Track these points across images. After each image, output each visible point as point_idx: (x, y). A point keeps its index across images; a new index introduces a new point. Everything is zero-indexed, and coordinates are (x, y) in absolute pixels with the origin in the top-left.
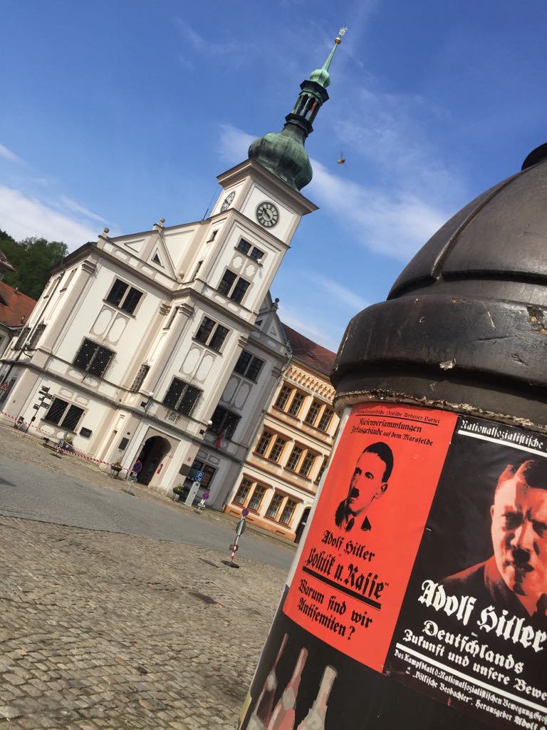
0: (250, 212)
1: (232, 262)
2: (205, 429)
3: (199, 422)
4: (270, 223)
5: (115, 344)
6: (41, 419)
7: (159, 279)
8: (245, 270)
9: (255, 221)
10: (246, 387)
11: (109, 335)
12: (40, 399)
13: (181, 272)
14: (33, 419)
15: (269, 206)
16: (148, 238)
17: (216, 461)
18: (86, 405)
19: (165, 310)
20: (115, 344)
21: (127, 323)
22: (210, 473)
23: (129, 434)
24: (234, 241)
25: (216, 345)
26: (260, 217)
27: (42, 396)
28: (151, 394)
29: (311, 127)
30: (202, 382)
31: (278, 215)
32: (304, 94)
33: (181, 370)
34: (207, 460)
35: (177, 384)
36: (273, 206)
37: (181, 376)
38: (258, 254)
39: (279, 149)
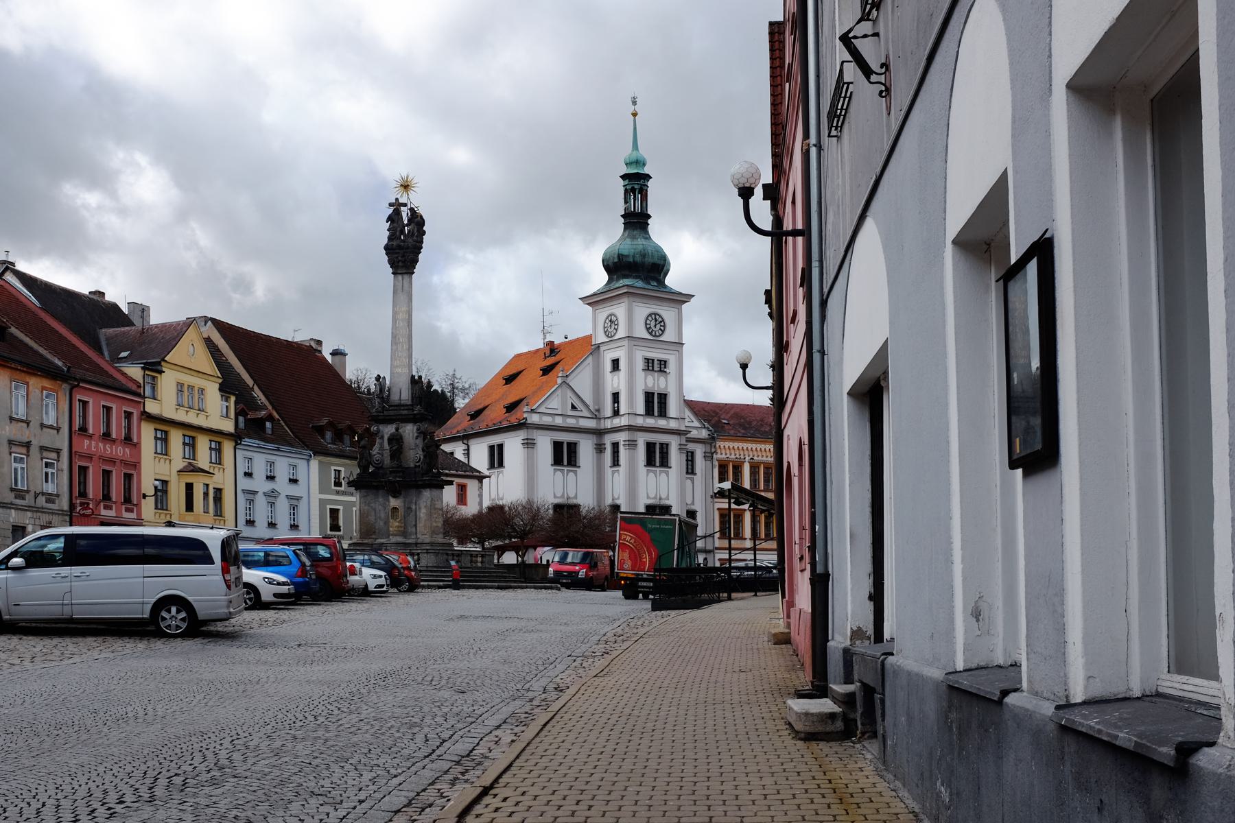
0: (641, 332)
5: (576, 497)
7: (585, 423)
24: (640, 364)
25: (665, 463)
33: (648, 497)
36: (655, 314)
39: (638, 259)
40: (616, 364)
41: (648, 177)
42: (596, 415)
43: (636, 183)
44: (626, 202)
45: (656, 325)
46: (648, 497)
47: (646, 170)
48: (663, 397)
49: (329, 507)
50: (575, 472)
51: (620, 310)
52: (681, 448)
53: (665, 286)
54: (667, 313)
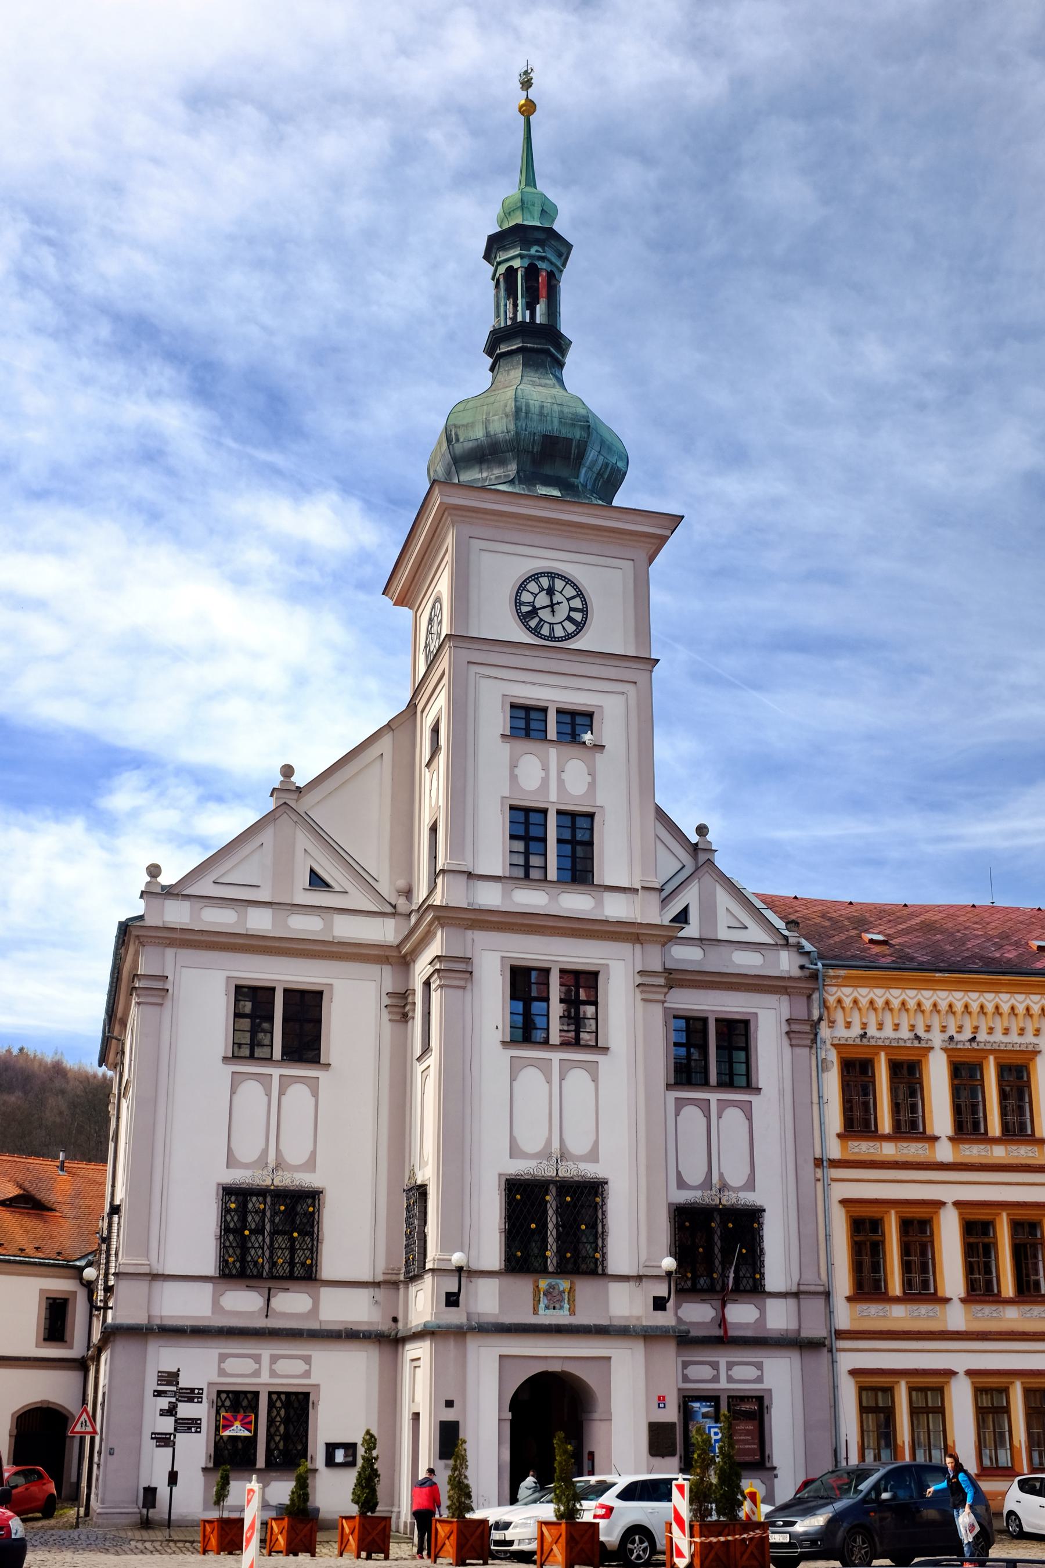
1: (513, 778)
3: (639, 1278)
4: (567, 624)
5: (311, 1164)
6: (205, 1470)
8: (561, 782)
10: (734, 1116)
11: (282, 1147)
12: (163, 1413)
13: (401, 883)
14: (173, 1478)
15: (545, 582)
16: (267, 836)
17: (751, 1372)
18: (307, 1374)
19: (400, 1007)
20: (311, 1164)
21: (315, 1094)
22: (749, 1416)
23: (449, 1404)
24: (494, 720)
26: (533, 623)
27: (164, 1403)
28: (457, 1258)
29: (561, 336)
30: (593, 1156)
31: (580, 594)
32: (502, 269)
33: (515, 1151)
34: (723, 1384)
35: (523, 1197)
36: (552, 576)
37: (521, 1168)
38: (576, 724)
46: (515, 1151)
50: (313, 1086)
54: (600, 578)
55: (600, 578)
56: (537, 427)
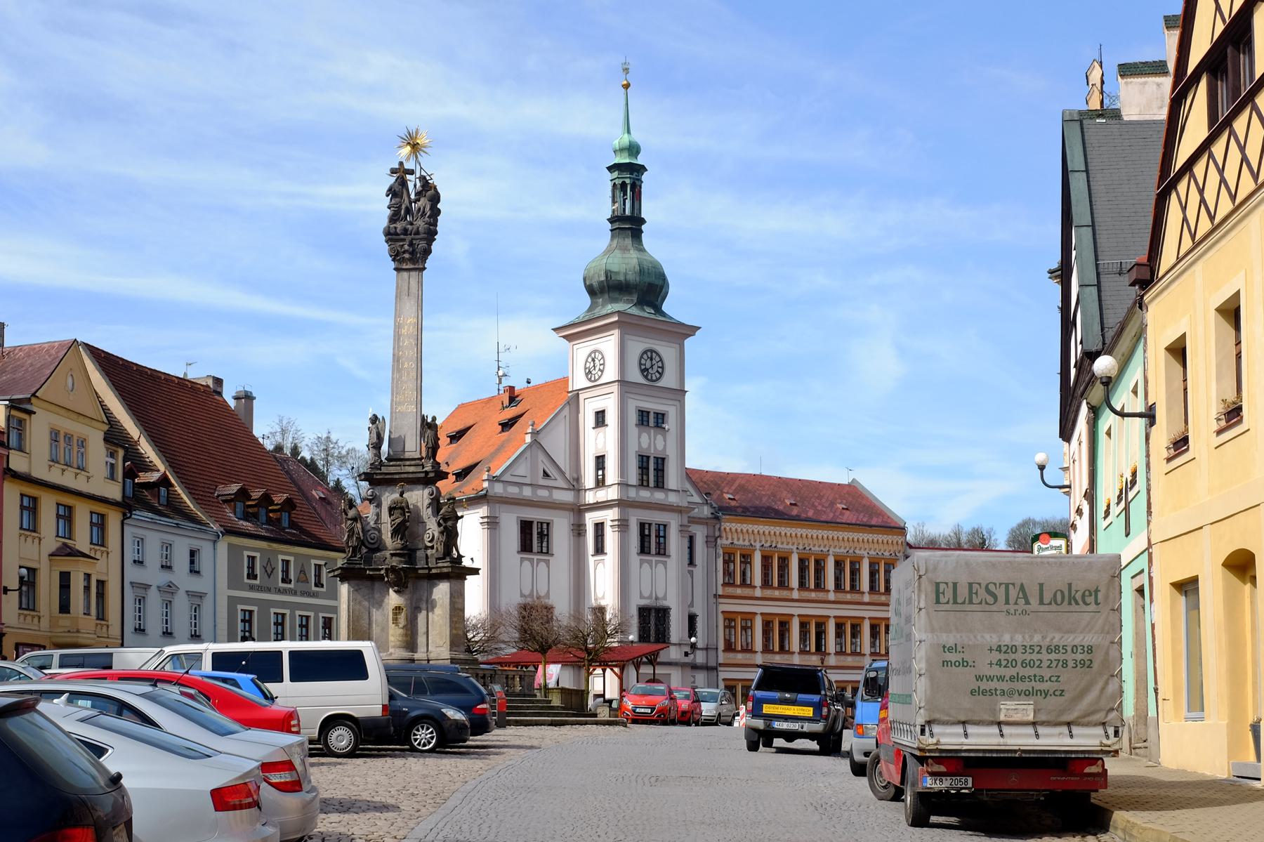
0: (635, 376)
2: (688, 649)
9: (643, 381)
24: (633, 418)
25: (662, 551)
30: (665, 598)
33: (642, 597)
35: (644, 612)
36: (652, 351)
37: (644, 602)
38: (660, 418)
39: (632, 277)
40: (600, 418)
41: (641, 169)
42: (576, 485)
43: (629, 177)
44: (614, 202)
45: (651, 366)
47: (640, 160)
48: (661, 462)
49: (240, 607)
50: (547, 562)
51: (609, 345)
52: (683, 529)
53: (663, 314)
55: (667, 352)
56: (647, 280)
